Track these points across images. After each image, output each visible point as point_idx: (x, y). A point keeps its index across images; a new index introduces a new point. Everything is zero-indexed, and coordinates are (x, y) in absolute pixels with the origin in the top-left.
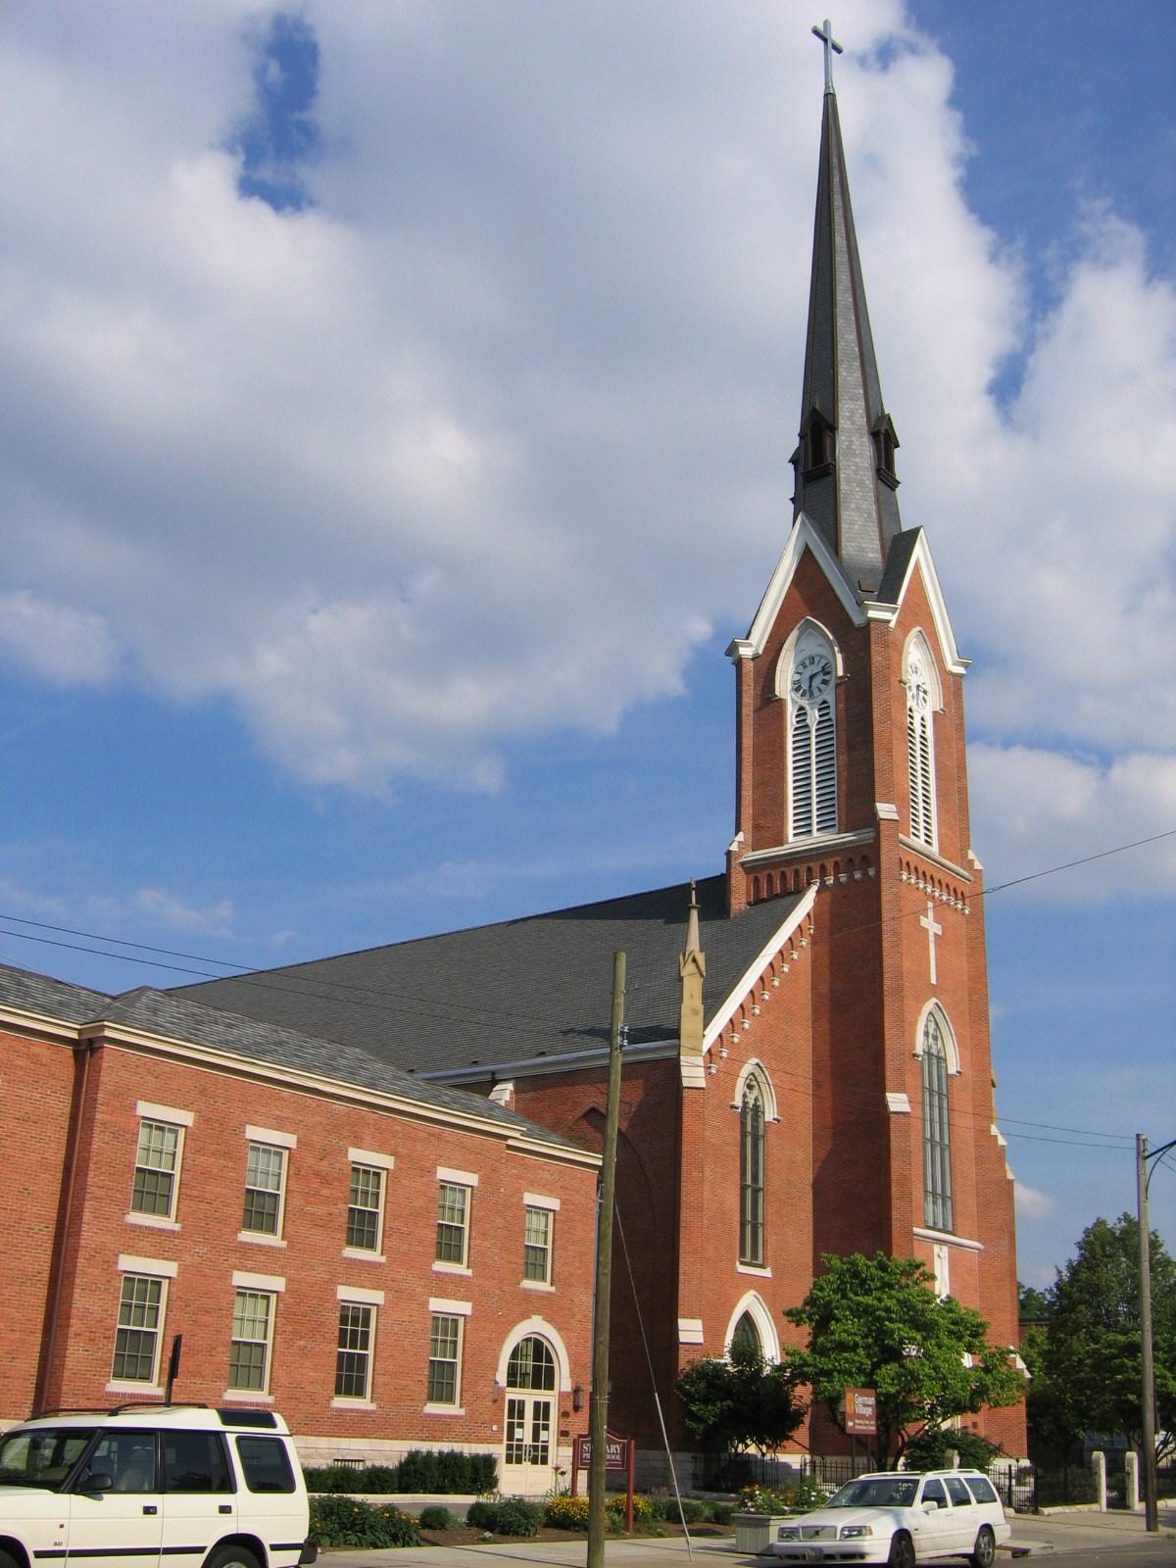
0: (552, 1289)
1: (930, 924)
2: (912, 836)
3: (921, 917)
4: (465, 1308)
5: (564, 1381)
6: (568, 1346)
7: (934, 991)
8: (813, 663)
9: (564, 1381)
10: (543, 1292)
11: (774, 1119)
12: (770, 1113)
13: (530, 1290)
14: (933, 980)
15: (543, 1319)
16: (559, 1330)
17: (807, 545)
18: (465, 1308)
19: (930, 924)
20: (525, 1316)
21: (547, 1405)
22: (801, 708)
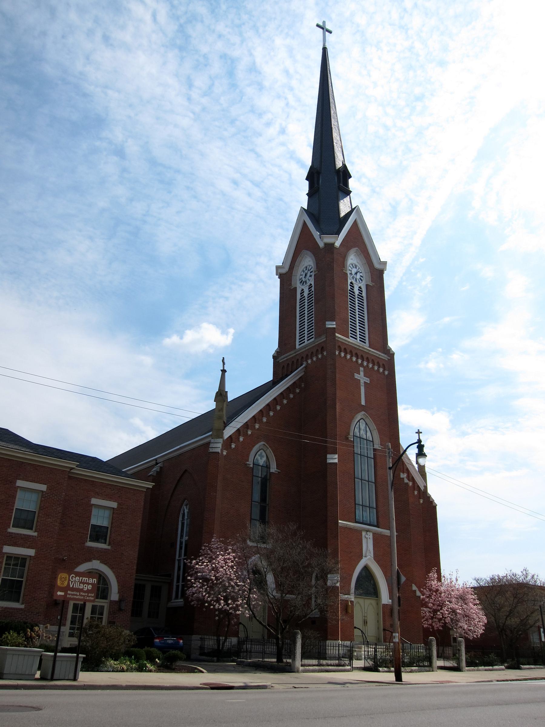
0: (109, 547)
1: (361, 377)
2: (350, 338)
3: (355, 374)
4: (31, 552)
5: (114, 596)
6: (117, 577)
7: (363, 408)
9: (114, 596)
10: (102, 549)
11: (276, 471)
12: (274, 469)
13: (91, 547)
14: (363, 403)
15: (101, 562)
16: (112, 568)
17: (305, 221)
18: (31, 552)
19: (361, 377)
20: (90, 560)
21: (102, 607)
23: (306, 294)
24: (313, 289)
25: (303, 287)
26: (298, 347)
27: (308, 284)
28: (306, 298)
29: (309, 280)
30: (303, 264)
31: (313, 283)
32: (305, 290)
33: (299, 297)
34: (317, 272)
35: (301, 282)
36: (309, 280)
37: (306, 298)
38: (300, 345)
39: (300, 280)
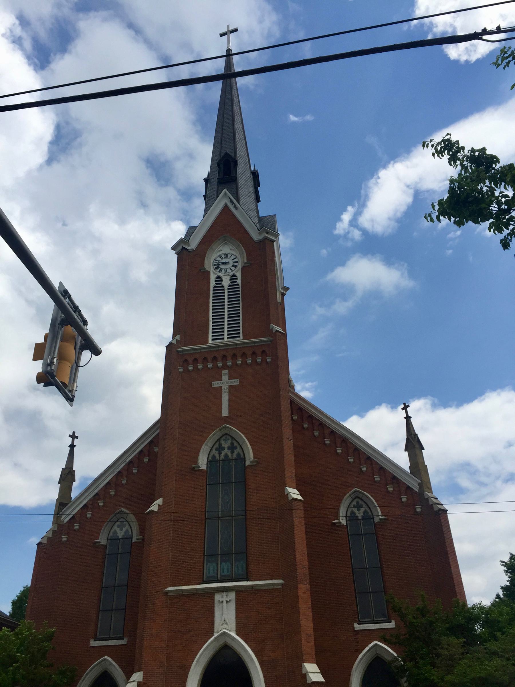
8: (227, 257)
22: (219, 277)
23: (226, 282)
24: (239, 281)
25: (220, 274)
26: (210, 341)
27: (231, 274)
28: (226, 288)
29: (231, 269)
30: (221, 248)
31: (239, 275)
32: (224, 278)
33: (212, 284)
34: (248, 265)
35: (216, 268)
36: (231, 269)
37: (226, 288)
38: (213, 340)
39: (214, 265)
